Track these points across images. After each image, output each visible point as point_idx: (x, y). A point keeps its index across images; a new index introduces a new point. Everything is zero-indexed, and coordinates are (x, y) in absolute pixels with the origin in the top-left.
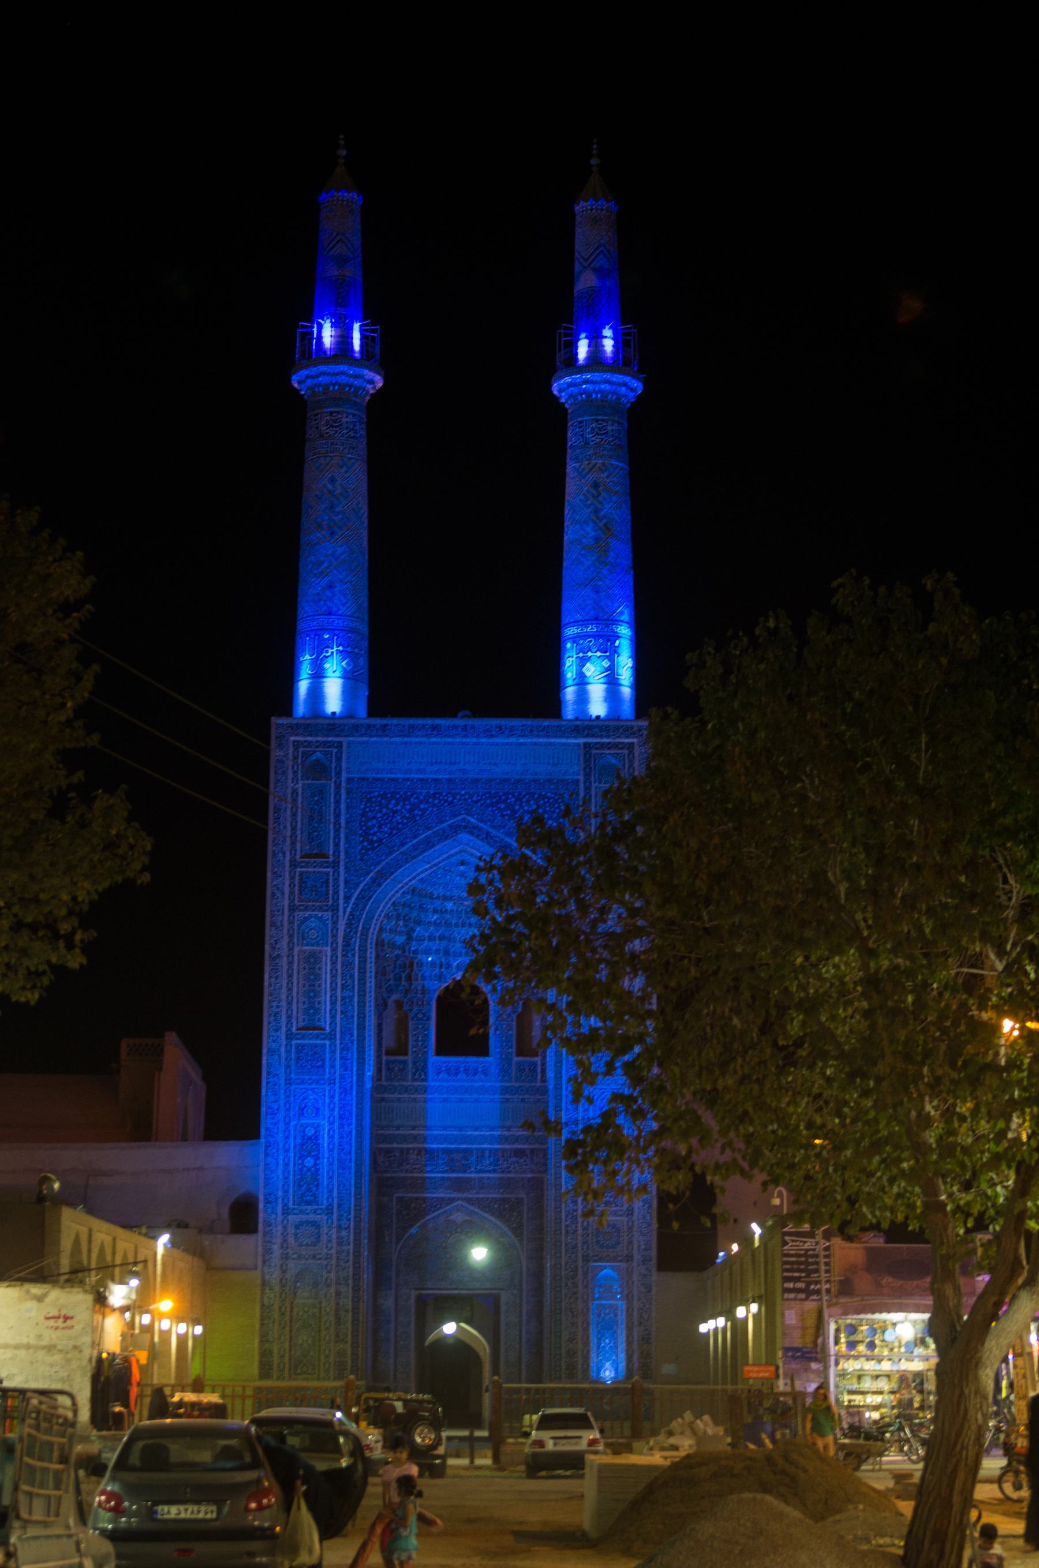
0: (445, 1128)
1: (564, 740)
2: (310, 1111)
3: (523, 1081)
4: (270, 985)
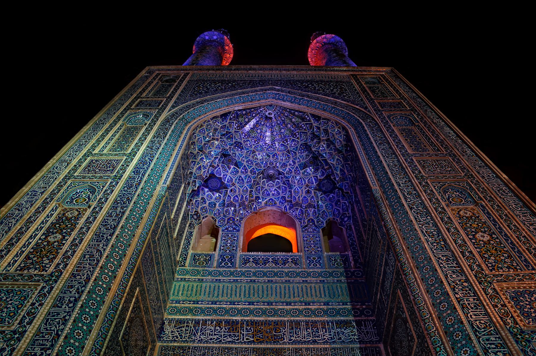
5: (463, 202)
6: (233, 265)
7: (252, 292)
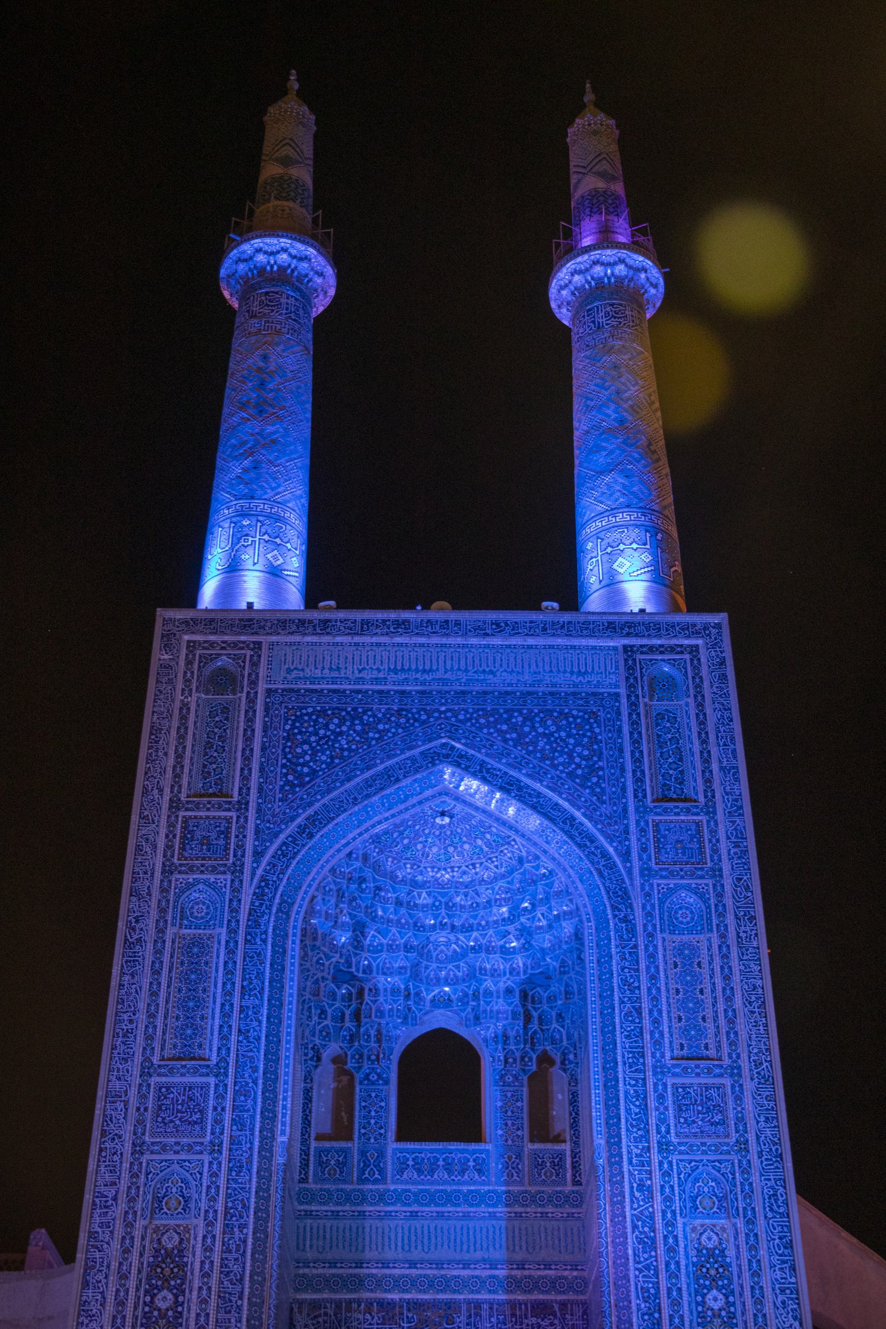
0: (413, 1264)
1: (592, 642)
2: (173, 1203)
3: (544, 1182)
4: (121, 986)
5: (715, 1209)
6: (382, 1171)
7: (413, 1238)
